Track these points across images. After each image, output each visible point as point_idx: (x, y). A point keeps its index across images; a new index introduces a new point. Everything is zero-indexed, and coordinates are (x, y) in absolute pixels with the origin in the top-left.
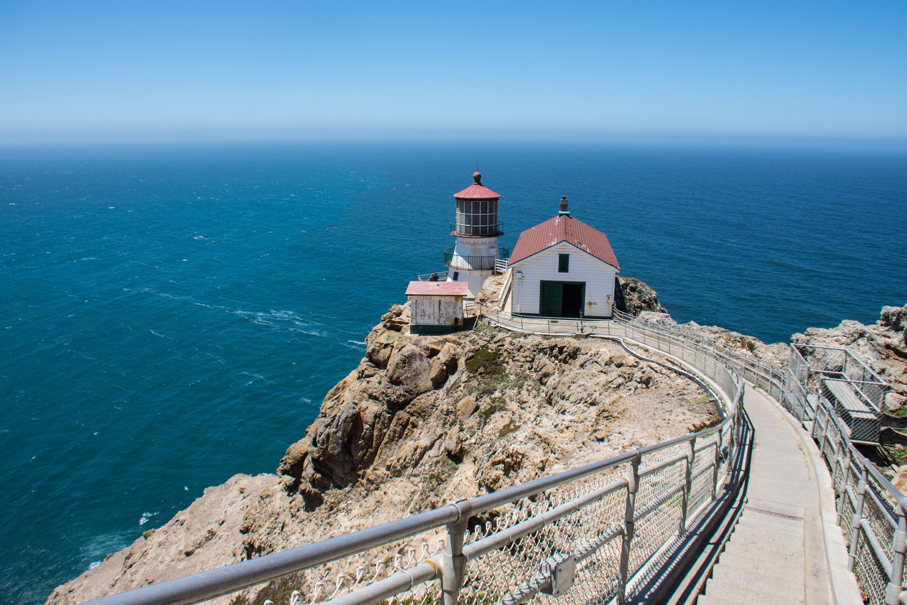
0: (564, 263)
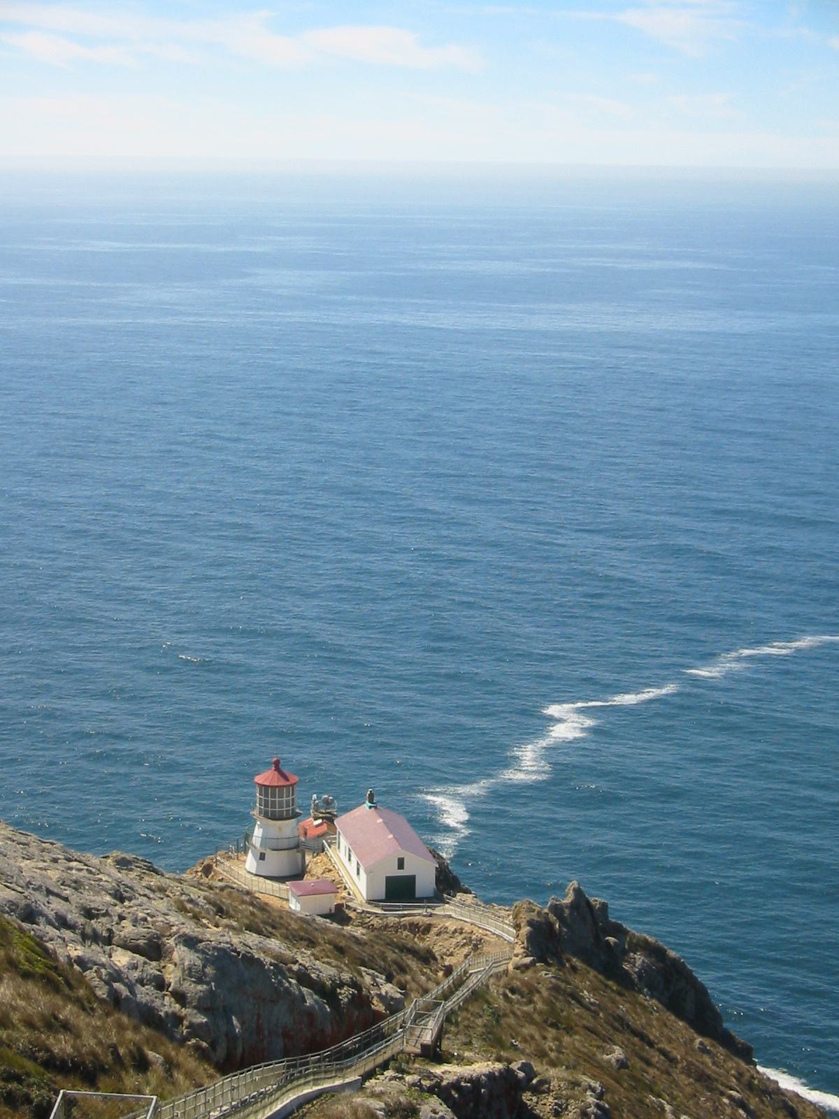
0: (401, 864)
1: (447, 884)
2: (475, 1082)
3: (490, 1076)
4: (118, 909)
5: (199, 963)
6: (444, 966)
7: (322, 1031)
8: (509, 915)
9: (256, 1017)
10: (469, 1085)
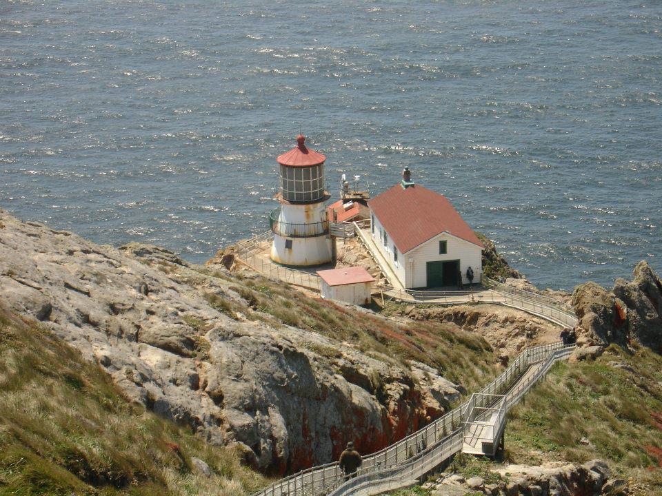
1: (494, 266)
2: (545, 485)
3: (561, 477)
4: (146, 304)
5: (237, 359)
6: (501, 358)
7: (374, 430)
8: (566, 301)
9: (301, 418)
10: (538, 487)
